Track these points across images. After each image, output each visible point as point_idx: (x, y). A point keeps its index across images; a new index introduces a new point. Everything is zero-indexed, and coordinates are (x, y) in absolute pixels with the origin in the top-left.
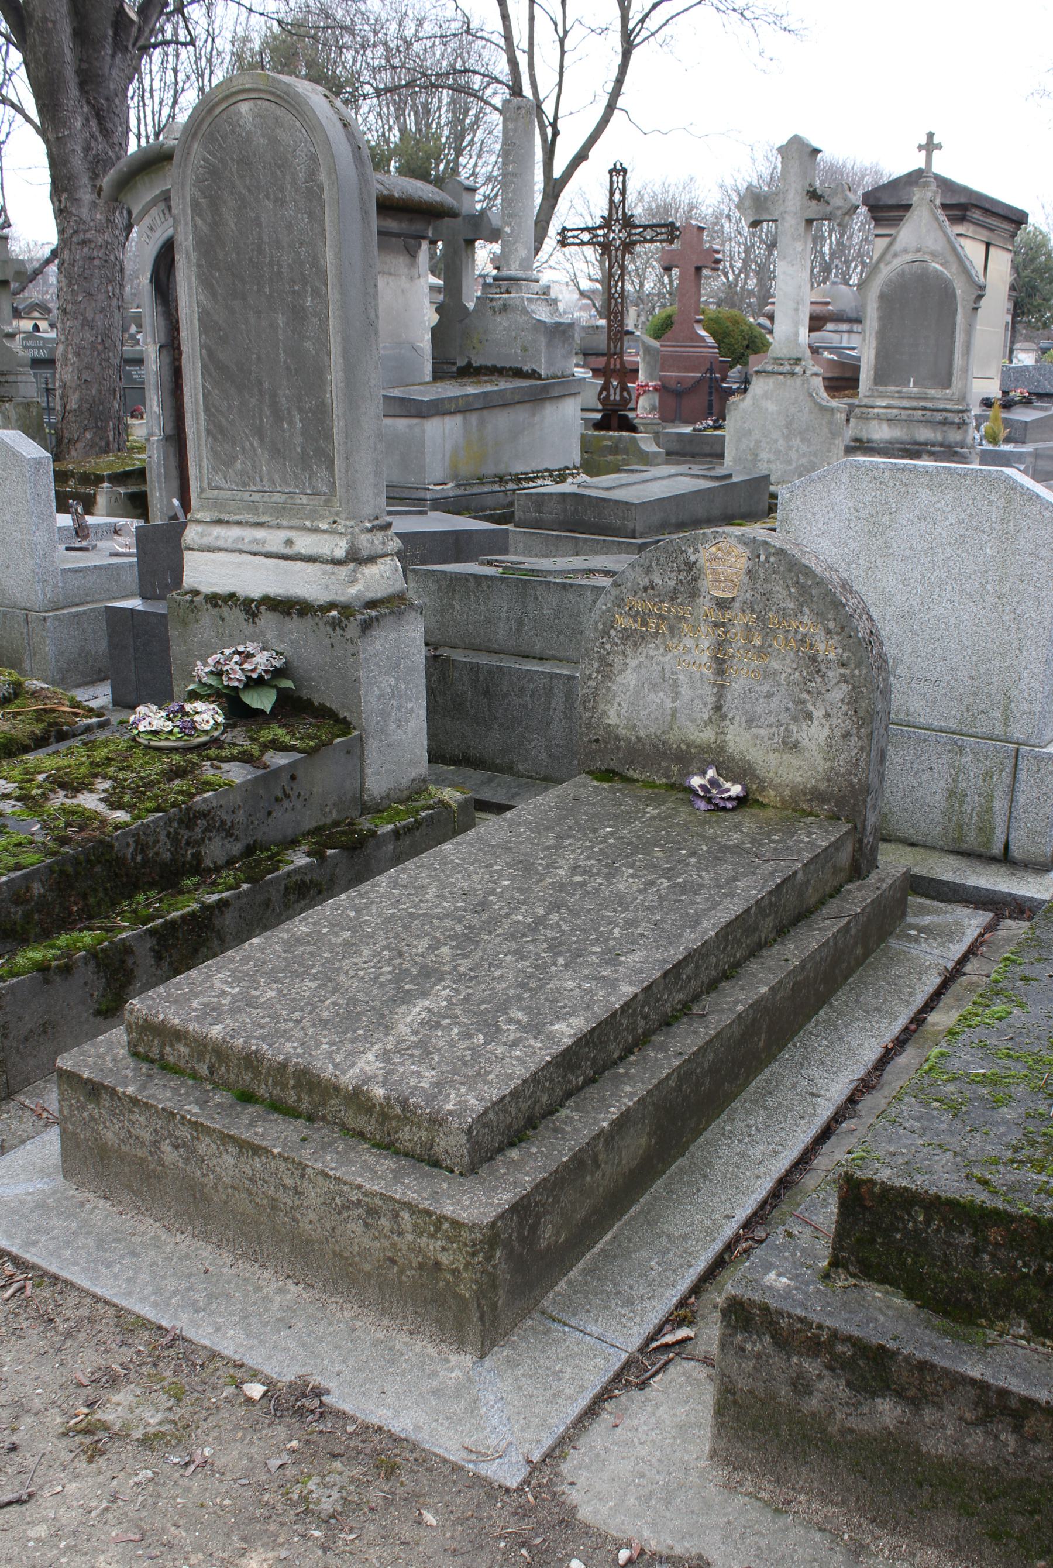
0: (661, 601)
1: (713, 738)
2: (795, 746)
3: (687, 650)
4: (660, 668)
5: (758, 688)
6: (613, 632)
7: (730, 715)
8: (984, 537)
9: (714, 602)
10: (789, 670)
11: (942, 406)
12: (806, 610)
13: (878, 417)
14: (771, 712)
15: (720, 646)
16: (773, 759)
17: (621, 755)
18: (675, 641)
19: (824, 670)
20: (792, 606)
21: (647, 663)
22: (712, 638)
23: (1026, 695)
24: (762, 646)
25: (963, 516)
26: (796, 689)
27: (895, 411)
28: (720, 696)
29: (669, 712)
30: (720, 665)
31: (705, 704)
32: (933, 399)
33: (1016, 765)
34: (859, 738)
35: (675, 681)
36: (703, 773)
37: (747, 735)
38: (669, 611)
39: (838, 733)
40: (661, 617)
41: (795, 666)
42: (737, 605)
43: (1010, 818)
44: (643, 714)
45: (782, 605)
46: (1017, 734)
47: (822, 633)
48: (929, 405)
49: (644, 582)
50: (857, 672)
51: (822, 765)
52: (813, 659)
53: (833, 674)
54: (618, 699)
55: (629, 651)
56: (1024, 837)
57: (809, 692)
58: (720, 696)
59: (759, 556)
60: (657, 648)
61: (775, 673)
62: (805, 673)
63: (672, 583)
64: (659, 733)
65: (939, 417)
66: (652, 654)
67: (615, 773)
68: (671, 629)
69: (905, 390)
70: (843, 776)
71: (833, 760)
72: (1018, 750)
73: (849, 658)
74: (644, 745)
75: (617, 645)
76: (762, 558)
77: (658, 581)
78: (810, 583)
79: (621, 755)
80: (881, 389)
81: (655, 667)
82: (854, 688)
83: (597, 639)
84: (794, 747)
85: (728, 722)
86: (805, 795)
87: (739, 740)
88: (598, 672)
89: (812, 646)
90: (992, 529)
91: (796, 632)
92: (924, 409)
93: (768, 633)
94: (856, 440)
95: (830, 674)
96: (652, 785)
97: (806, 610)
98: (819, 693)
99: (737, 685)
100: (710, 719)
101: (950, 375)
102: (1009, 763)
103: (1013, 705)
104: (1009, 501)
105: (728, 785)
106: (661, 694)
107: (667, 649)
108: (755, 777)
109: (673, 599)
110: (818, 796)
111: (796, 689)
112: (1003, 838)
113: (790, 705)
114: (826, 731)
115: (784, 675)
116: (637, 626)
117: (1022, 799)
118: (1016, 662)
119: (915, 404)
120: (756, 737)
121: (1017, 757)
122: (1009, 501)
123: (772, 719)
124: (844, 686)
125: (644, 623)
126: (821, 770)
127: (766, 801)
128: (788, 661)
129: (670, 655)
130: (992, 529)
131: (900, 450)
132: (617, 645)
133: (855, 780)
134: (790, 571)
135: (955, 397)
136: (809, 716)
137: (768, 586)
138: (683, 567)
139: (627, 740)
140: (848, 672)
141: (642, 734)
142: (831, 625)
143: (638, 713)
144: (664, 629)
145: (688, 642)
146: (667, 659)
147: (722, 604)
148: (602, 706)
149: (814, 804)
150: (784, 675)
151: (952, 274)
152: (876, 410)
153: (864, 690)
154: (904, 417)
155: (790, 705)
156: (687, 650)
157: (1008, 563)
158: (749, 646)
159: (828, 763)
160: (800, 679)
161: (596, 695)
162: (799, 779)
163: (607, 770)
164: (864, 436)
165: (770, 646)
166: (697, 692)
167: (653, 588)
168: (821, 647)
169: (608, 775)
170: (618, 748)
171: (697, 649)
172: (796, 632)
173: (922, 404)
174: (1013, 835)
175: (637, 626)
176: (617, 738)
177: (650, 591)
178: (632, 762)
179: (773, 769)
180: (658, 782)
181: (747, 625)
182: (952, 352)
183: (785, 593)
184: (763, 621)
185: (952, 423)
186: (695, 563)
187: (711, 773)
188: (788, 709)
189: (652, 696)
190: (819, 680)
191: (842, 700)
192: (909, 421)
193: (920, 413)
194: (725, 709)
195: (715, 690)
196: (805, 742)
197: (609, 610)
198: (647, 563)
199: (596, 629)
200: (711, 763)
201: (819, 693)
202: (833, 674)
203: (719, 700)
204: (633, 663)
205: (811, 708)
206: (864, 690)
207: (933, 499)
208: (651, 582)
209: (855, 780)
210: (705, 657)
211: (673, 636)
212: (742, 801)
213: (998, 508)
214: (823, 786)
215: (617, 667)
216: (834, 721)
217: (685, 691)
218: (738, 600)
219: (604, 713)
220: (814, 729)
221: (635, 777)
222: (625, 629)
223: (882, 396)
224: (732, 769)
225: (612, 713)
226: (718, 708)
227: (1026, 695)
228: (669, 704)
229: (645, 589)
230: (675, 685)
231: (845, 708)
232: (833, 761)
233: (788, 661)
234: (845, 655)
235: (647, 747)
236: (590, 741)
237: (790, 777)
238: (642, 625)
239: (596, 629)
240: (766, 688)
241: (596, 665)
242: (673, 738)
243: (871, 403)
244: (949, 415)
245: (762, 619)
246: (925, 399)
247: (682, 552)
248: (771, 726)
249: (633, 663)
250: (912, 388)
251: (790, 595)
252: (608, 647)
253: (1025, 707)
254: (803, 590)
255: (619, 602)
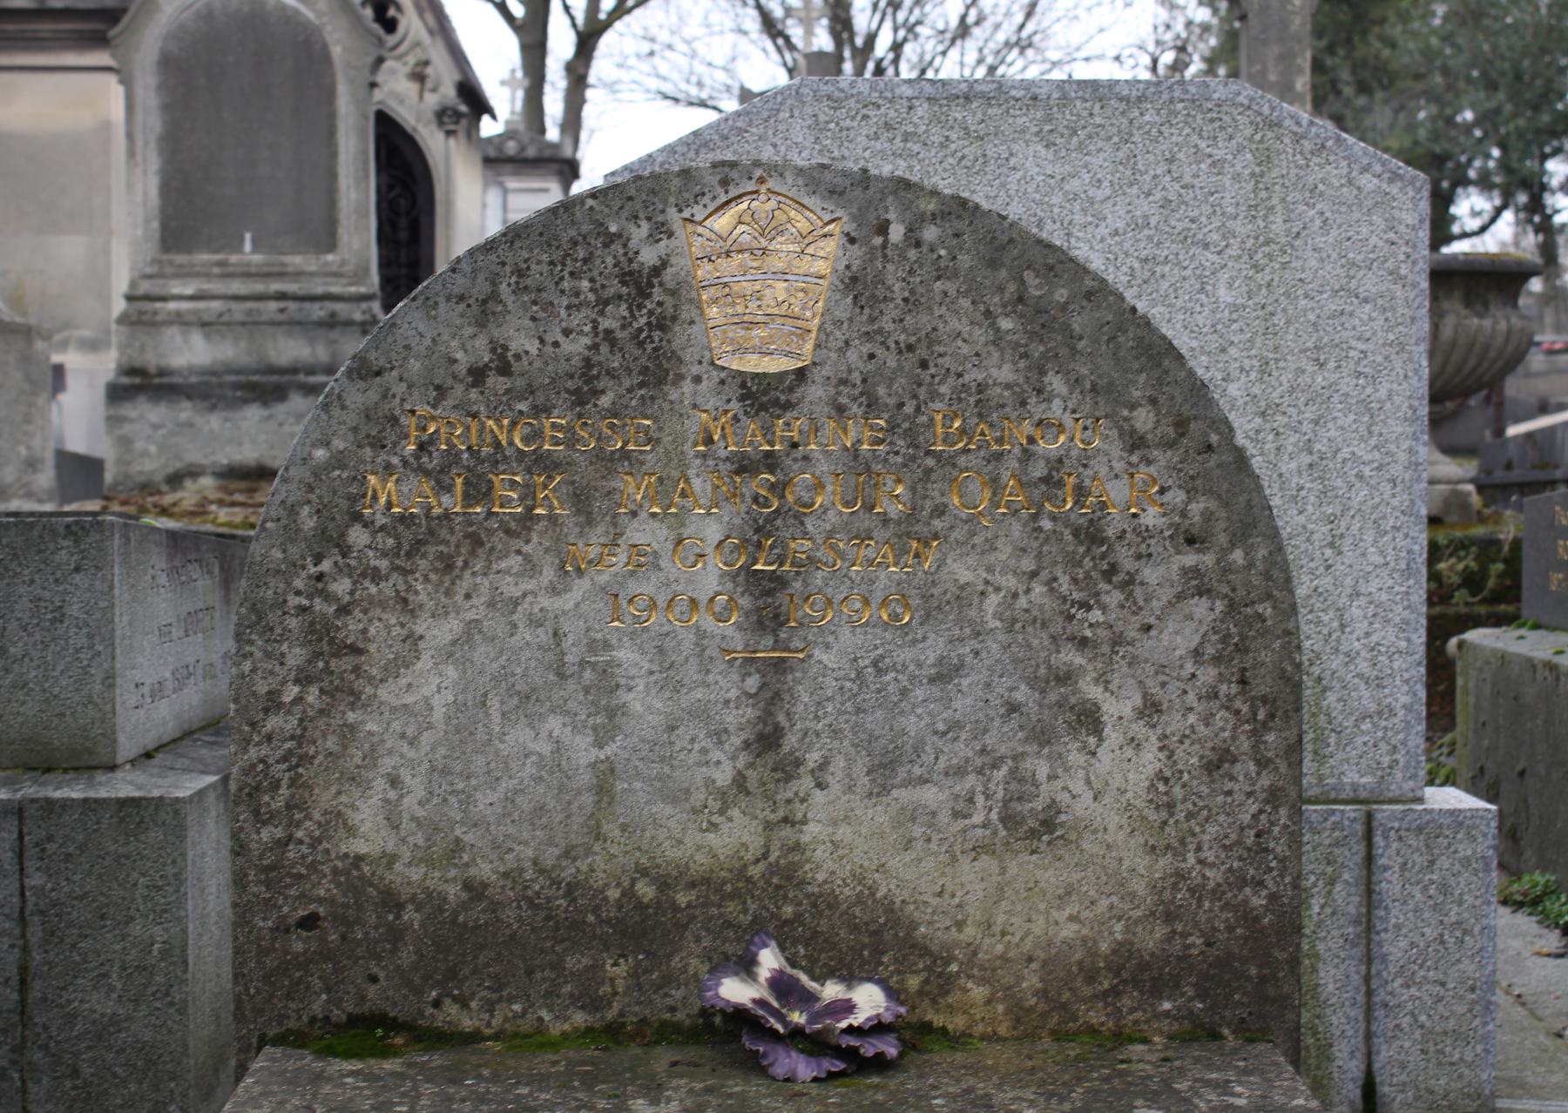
0: (537, 411)
1: (755, 843)
2: (1048, 825)
3: (642, 561)
4: (543, 635)
5: (906, 655)
6: (358, 536)
7: (813, 758)
8: (1210, 257)
9: (733, 391)
10: (1010, 582)
11: (320, 290)
12: (1056, 383)
13: (179, 320)
14: (956, 725)
15: (760, 531)
16: (973, 878)
17: (406, 956)
18: (598, 535)
19: (1128, 564)
20: (1006, 374)
21: (495, 624)
22: (735, 513)
23: (1363, 666)
24: (912, 516)
25: (1144, 207)
26: (1039, 639)
27: (216, 305)
28: (771, 699)
29: (586, 778)
30: (767, 598)
31: (719, 736)
32: (298, 275)
33: (1369, 858)
34: (1263, 763)
35: (605, 671)
36: (746, 966)
37: (878, 815)
38: (572, 441)
39: (1189, 758)
40: (543, 463)
41: (1028, 564)
42: (815, 392)
43: (1369, 1009)
44: (486, 801)
45: (974, 376)
46: (1351, 777)
47: (1116, 449)
48: (291, 287)
49: (472, 349)
50: (1238, 556)
51: (1143, 869)
52: (1091, 535)
53: (1160, 575)
54: (387, 764)
55: (423, 593)
56: (1415, 1056)
57: (1083, 643)
58: (771, 699)
59: (883, 229)
60: (531, 567)
61: (963, 596)
62: (1064, 584)
63: (576, 347)
64: (550, 856)
65: (318, 311)
66: (510, 588)
67: (392, 1025)
68: (581, 500)
69: (234, 258)
70: (1217, 893)
71: (1178, 850)
72: (1369, 816)
73: (1208, 516)
74: (495, 906)
75: (376, 576)
76: (897, 232)
77: (522, 341)
78: (1061, 294)
79: (406, 956)
80: (180, 258)
81: (525, 634)
82: (1232, 607)
83: (296, 566)
84: (1042, 828)
85: (807, 783)
86: (1091, 979)
87: (846, 835)
88: (304, 679)
89: (1081, 492)
90: (1228, 235)
91: (1027, 456)
92: (282, 296)
93: (927, 466)
94: (132, 371)
95: (1150, 574)
96: (537, 1040)
97: (1056, 383)
98: (1117, 641)
99: (833, 651)
100: (740, 781)
101: (332, 223)
102: (1351, 856)
103: (1331, 698)
104: (1265, 158)
105: (832, 991)
106: (554, 724)
107: (569, 569)
108: (912, 948)
109: (581, 399)
110: (1135, 974)
111: (1039, 639)
112: (1355, 1068)
113: (1022, 694)
114: (1151, 760)
115: (993, 600)
116: (452, 503)
117: (1395, 948)
118: (1326, 582)
119: (258, 287)
120: (910, 815)
121: (1369, 836)
122: (1265, 158)
123: (962, 750)
124: (1200, 608)
125: (478, 491)
126: (1139, 887)
127: (957, 1023)
128: (1004, 552)
129: (581, 586)
130: (1228, 235)
131: (237, 386)
132: (376, 576)
133: (1258, 901)
134: (993, 264)
135: (349, 268)
136: (1089, 720)
137: (924, 321)
138: (615, 286)
139: (431, 902)
140: (1208, 559)
141: (485, 870)
142: (1143, 419)
143: (467, 800)
144: (552, 499)
145: (647, 533)
146: (568, 601)
147: (763, 396)
148: (324, 798)
149: (1126, 1002)
150: (993, 600)
151: (319, 14)
152: (172, 306)
153: (1266, 609)
154: (238, 317)
155: (1022, 694)
156: (642, 561)
157: (1279, 319)
158: (866, 522)
159: (1165, 863)
160: (1049, 603)
161: (297, 759)
162: (1068, 931)
163: (354, 1021)
164: (151, 360)
165: (940, 511)
166: (686, 700)
167: (505, 370)
168: (1117, 492)
169: (365, 1033)
170: (396, 935)
171: (682, 554)
172: (1027, 456)
173: (276, 286)
174: (1384, 1054)
175: (452, 503)
176: (391, 900)
177: (495, 382)
178: (452, 974)
179: (974, 912)
180: (557, 1029)
181: (854, 452)
182: (333, 176)
183: (980, 335)
184: (911, 435)
185: (349, 323)
186: (657, 271)
187: (769, 960)
188: (1013, 708)
189: (520, 735)
190: (1114, 598)
191: (1197, 653)
192: (251, 324)
193: (273, 306)
194: (790, 741)
195: (752, 683)
196: (1083, 806)
197: (338, 461)
198: (482, 288)
199: (291, 532)
200: (757, 931)
201: (1117, 641)
202: (1160, 575)
203: (768, 713)
204: (439, 632)
205: (1094, 692)
206: (1266, 609)
207: (1059, 170)
208: (499, 350)
209: (1258, 901)
210: (710, 577)
211: (590, 522)
212: (913, 1035)
213: (1237, 177)
214: (1151, 939)
215: (380, 652)
216: (1174, 723)
217: (643, 703)
218: (818, 374)
219: (337, 819)
220: (1106, 759)
221: (468, 1024)
222: (406, 519)
223: (183, 274)
224: (861, 935)
225: (366, 814)
226: (766, 740)
227: (1363, 666)
228: (583, 752)
229: (478, 375)
230: (607, 681)
231: (1208, 675)
232: (1178, 850)
233: (1004, 552)
234: (1196, 508)
235: (509, 914)
236: (282, 929)
237: (1038, 928)
238: (469, 500)
239: (291, 532)
240: (934, 648)
241: (296, 656)
242: (603, 867)
243: (156, 291)
244: (339, 307)
245: (907, 429)
246: (281, 275)
247: (610, 239)
248: (959, 772)
249: (439, 632)
250: (249, 253)
251: (998, 339)
252: (341, 587)
253: (1365, 698)
254: (1042, 321)
255: (380, 430)
